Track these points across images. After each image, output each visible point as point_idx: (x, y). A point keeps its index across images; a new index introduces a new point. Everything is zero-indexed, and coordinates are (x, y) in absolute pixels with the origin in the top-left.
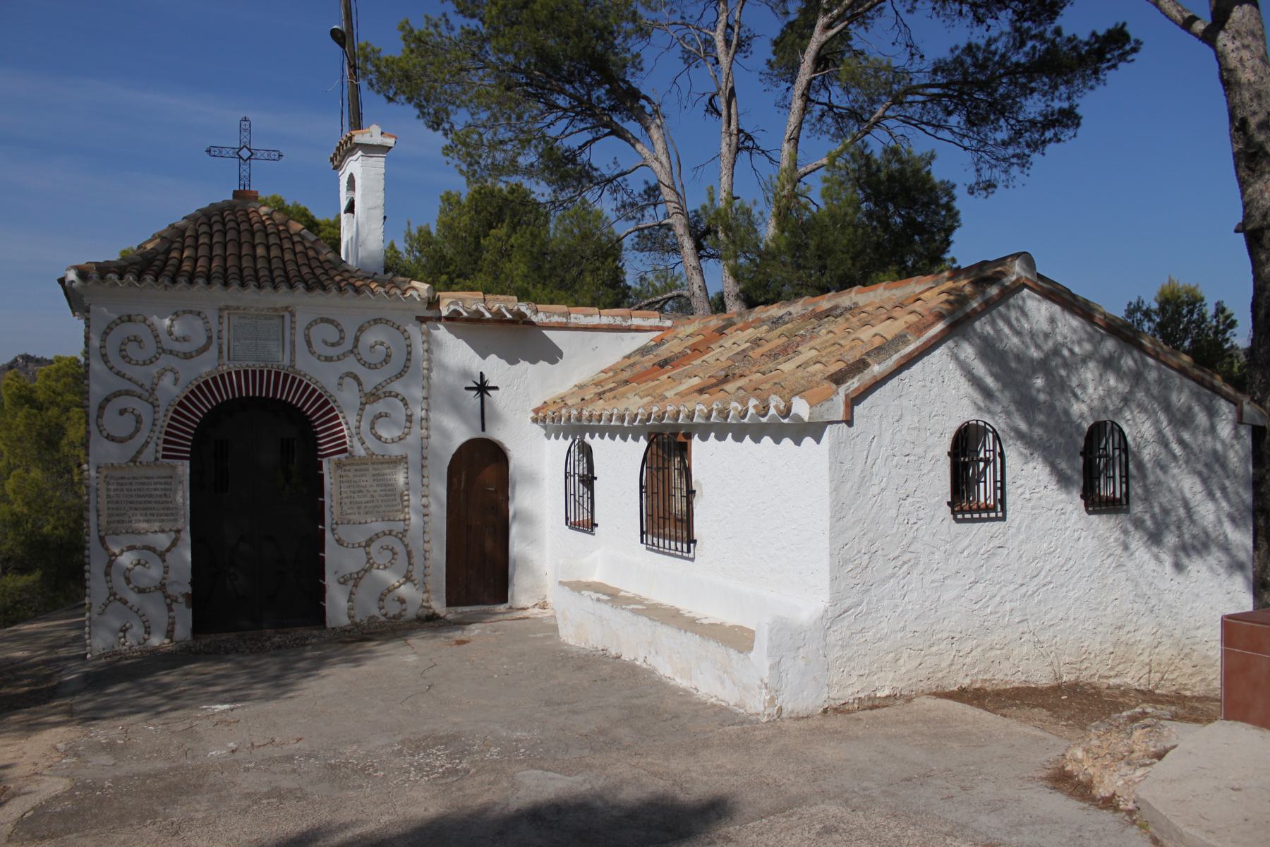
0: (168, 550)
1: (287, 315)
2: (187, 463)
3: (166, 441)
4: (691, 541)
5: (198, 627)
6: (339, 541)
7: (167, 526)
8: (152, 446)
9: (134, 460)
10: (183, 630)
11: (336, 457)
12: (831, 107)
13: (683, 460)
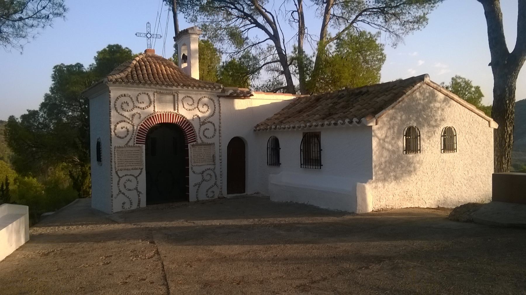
0: (138, 176)
1: (176, 95)
2: (144, 145)
3: (137, 138)
4: (321, 165)
5: (149, 201)
6: (194, 172)
7: (138, 167)
8: (132, 140)
9: (127, 144)
10: (143, 204)
11: (192, 143)
12: (334, 15)
13: (317, 139)
